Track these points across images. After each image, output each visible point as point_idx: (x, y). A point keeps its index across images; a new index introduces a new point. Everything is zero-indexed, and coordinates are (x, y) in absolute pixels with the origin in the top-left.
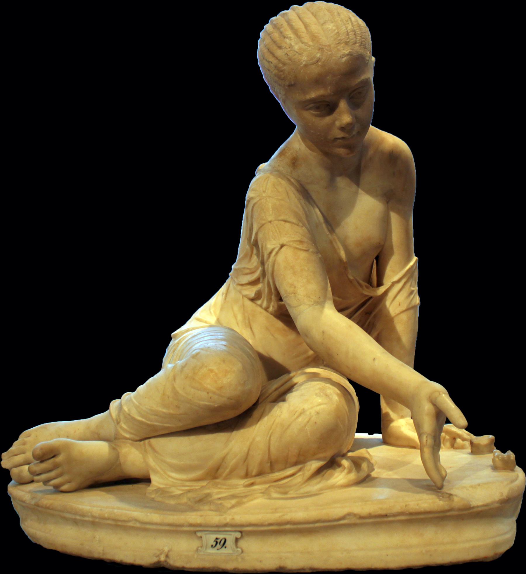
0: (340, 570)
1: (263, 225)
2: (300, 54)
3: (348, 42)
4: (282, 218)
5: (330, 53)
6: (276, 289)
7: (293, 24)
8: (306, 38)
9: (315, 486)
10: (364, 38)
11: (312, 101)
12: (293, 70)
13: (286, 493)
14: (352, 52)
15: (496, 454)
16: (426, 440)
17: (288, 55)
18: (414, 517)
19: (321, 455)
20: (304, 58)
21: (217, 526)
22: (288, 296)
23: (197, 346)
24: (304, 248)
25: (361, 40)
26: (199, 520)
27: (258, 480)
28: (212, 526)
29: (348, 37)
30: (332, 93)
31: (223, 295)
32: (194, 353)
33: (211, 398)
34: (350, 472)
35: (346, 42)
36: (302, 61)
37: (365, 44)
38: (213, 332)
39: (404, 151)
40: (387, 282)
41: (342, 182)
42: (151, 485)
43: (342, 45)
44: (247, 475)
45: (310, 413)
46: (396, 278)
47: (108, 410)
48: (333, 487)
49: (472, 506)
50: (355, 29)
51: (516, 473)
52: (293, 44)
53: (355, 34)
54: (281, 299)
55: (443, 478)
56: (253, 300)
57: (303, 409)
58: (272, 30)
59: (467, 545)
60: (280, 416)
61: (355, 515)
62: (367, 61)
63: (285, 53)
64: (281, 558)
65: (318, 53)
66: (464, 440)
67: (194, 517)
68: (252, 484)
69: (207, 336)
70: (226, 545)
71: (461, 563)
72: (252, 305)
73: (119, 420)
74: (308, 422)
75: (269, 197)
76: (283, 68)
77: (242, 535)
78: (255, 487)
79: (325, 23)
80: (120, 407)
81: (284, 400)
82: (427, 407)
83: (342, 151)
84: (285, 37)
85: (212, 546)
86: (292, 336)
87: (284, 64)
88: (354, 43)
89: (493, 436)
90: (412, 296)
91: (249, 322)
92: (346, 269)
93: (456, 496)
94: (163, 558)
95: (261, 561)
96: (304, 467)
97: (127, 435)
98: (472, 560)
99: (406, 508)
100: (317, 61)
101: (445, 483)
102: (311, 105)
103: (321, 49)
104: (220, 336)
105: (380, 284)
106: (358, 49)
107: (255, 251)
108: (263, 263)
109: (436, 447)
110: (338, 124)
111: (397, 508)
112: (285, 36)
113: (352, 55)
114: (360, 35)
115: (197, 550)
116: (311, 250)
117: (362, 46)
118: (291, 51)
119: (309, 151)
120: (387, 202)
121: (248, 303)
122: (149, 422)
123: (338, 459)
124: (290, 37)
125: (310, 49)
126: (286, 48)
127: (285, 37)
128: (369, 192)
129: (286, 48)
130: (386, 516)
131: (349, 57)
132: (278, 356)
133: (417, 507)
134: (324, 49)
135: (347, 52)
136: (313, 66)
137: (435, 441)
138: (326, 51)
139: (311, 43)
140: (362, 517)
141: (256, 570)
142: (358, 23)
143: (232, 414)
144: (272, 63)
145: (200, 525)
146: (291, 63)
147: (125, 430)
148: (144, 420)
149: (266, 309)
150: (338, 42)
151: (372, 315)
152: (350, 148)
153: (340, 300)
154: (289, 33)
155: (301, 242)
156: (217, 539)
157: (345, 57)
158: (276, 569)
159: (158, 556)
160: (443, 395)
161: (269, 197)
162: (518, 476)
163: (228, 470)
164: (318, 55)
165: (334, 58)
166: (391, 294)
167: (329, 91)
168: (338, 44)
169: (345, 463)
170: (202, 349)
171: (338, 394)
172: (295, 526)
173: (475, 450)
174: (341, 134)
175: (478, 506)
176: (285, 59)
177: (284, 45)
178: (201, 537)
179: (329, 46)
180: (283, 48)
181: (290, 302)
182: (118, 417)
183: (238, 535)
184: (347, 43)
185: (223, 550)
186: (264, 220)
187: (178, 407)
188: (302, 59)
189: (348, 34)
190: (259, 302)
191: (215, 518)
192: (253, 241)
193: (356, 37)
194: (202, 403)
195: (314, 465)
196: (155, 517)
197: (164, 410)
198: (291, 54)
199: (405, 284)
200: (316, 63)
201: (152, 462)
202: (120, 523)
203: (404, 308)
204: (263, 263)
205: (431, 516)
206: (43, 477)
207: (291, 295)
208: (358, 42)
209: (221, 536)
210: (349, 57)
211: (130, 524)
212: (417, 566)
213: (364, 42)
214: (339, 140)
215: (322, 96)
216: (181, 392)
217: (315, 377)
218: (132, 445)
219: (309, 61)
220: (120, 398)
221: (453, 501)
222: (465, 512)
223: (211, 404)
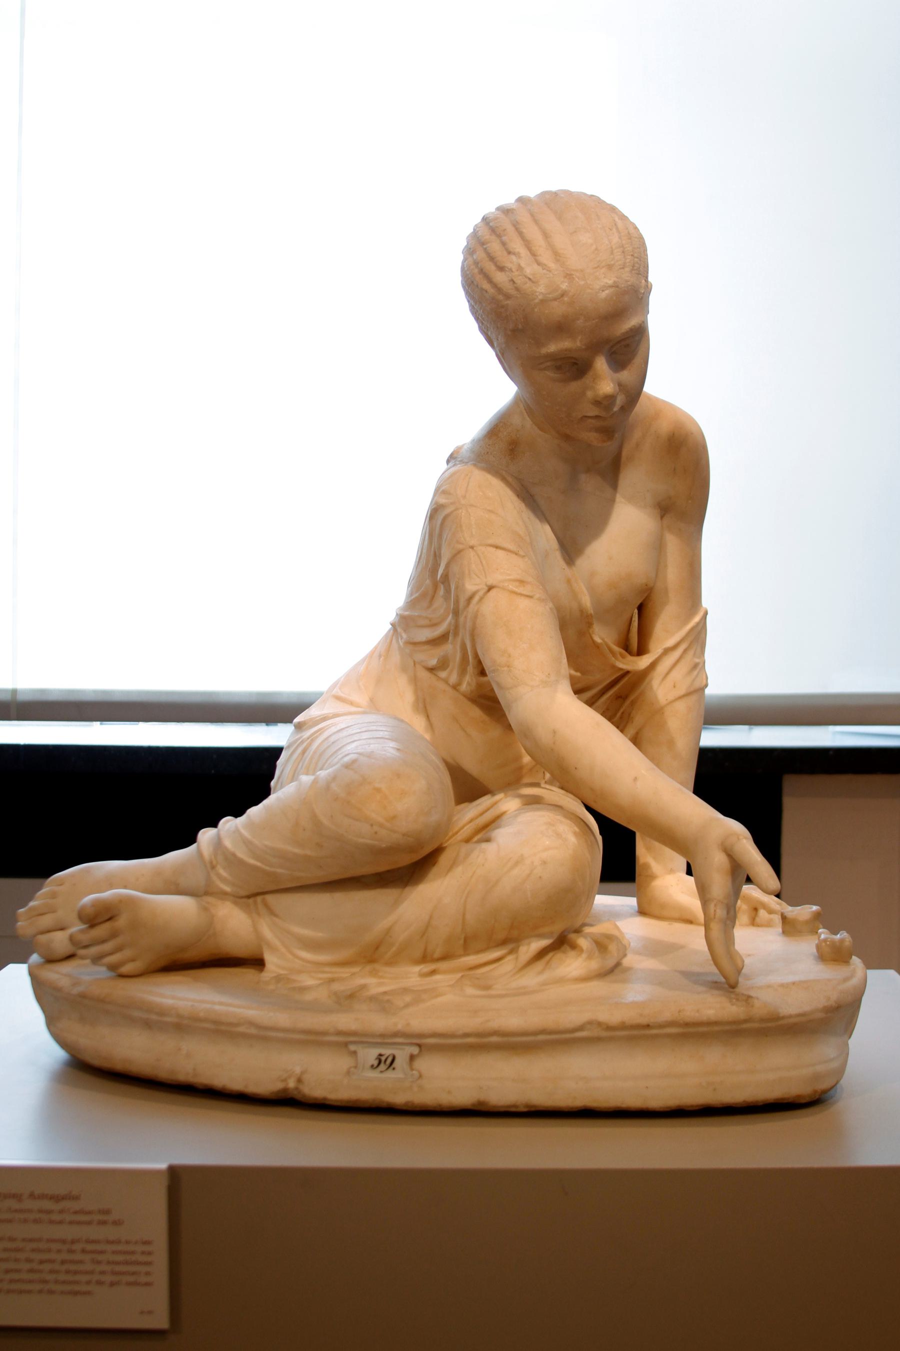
0: (572, 1108)
1: (460, 552)
2: (533, 282)
3: (613, 265)
4: (490, 542)
5: (582, 283)
6: (476, 656)
7: (524, 231)
8: (546, 257)
9: (531, 979)
10: (637, 258)
11: (552, 357)
12: (522, 306)
13: (488, 988)
15: (823, 936)
16: (715, 911)
17: (514, 282)
18: (691, 1030)
19: (546, 930)
20: (541, 290)
21: (382, 1036)
22: (498, 670)
23: (350, 748)
24: (525, 593)
25: (632, 261)
26: (354, 1026)
27: (443, 965)
28: (373, 1035)
29: (612, 256)
30: (584, 347)
31: (380, 659)
32: (346, 759)
33: (376, 833)
34: (590, 957)
35: (609, 265)
36: (537, 294)
37: (639, 268)
38: (373, 724)
39: (692, 434)
40: (656, 649)
41: (589, 483)
42: (266, 969)
43: (603, 270)
44: (424, 958)
45: (532, 863)
46: (670, 642)
47: (194, 846)
48: (561, 981)
49: (781, 1015)
50: (624, 242)
51: (853, 967)
52: (523, 264)
53: (623, 252)
54: (483, 673)
55: (739, 971)
56: (431, 670)
57: (522, 855)
58: (487, 237)
60: (483, 865)
61: (599, 1024)
62: (642, 295)
63: (510, 279)
64: (481, 1088)
65: (563, 282)
66: (771, 912)
67: (345, 1021)
68: (433, 972)
69: (366, 731)
70: (395, 1065)
71: (761, 1104)
72: (430, 678)
73: (214, 862)
74: (529, 875)
75: (472, 505)
76: (506, 303)
77: (420, 1051)
78: (437, 977)
79: (575, 232)
80: (218, 843)
81: (488, 840)
82: (719, 859)
83: (592, 437)
84: (509, 253)
85: (372, 1066)
86: (496, 732)
87: (508, 297)
88: (621, 267)
89: (818, 907)
90: (695, 673)
91: (425, 707)
92: (590, 625)
93: (758, 999)
94: (291, 1084)
95: (449, 1092)
96: (518, 947)
97: (227, 889)
98: (777, 1099)
99: (679, 1014)
100: (562, 295)
101: (740, 979)
102: (548, 364)
103: (569, 276)
104: (381, 733)
105: (641, 650)
106: (628, 277)
107: (441, 591)
108: (456, 613)
109: (728, 922)
110: (590, 394)
111: (666, 1016)
112: (512, 250)
113: (617, 287)
114: (632, 253)
115: (348, 1073)
116: (537, 596)
117: (633, 272)
118: (519, 275)
119: (540, 432)
120: (662, 517)
121: (424, 674)
122: (267, 868)
123: (572, 936)
124: (519, 253)
125: (551, 275)
126: (512, 271)
127: (509, 253)
129: (511, 270)
130: (648, 1026)
131: (612, 290)
132: (471, 764)
133: (697, 1014)
134: (574, 276)
135: (610, 282)
136: (556, 303)
137: (728, 913)
138: (577, 279)
139: (552, 265)
140: (609, 1028)
141: (440, 1105)
142: (629, 233)
143: (406, 860)
144: (486, 291)
145: (354, 1033)
146: (518, 296)
147: (224, 880)
148: (259, 864)
149: (455, 687)
150: (596, 266)
151: (628, 702)
152: (608, 432)
153: (578, 674)
154: (517, 246)
155: (522, 582)
156: (381, 1055)
158: (473, 1105)
159: (285, 1080)
160: (745, 841)
161: (472, 505)
162: (854, 971)
163: (394, 949)
164: (564, 286)
165: (590, 291)
166: (662, 668)
167: (578, 344)
168: (596, 268)
169: (583, 942)
170: (360, 754)
171: (575, 833)
172: (505, 1039)
173: (789, 927)
174: (594, 411)
175: (790, 1016)
176: (508, 287)
177: (509, 265)
178: (355, 1053)
179: (582, 271)
180: (507, 269)
181: (500, 679)
182: (213, 857)
183: (415, 1050)
184: (610, 267)
185: (390, 1074)
186: (462, 544)
187: (319, 845)
188: (538, 290)
189: (612, 253)
190: (443, 674)
191: (379, 1023)
192: (441, 576)
193: (624, 256)
194: (361, 840)
195: (537, 945)
196: (282, 1019)
197: (297, 850)
198: (519, 281)
199: (685, 651)
200: (559, 299)
201: (267, 932)
202: (223, 1028)
203: (682, 691)
204: (456, 613)
205: (716, 1028)
206: (94, 950)
207: (503, 669)
208: (628, 264)
209: (387, 1052)
210: (612, 290)
211: (241, 1029)
212: (692, 1106)
213: (638, 263)
214: (590, 420)
215: (566, 350)
216: (325, 821)
217: (534, 802)
218: (235, 903)
219: (549, 294)
220: (215, 825)
221: (752, 1006)
222: (769, 1025)
223: (375, 843)
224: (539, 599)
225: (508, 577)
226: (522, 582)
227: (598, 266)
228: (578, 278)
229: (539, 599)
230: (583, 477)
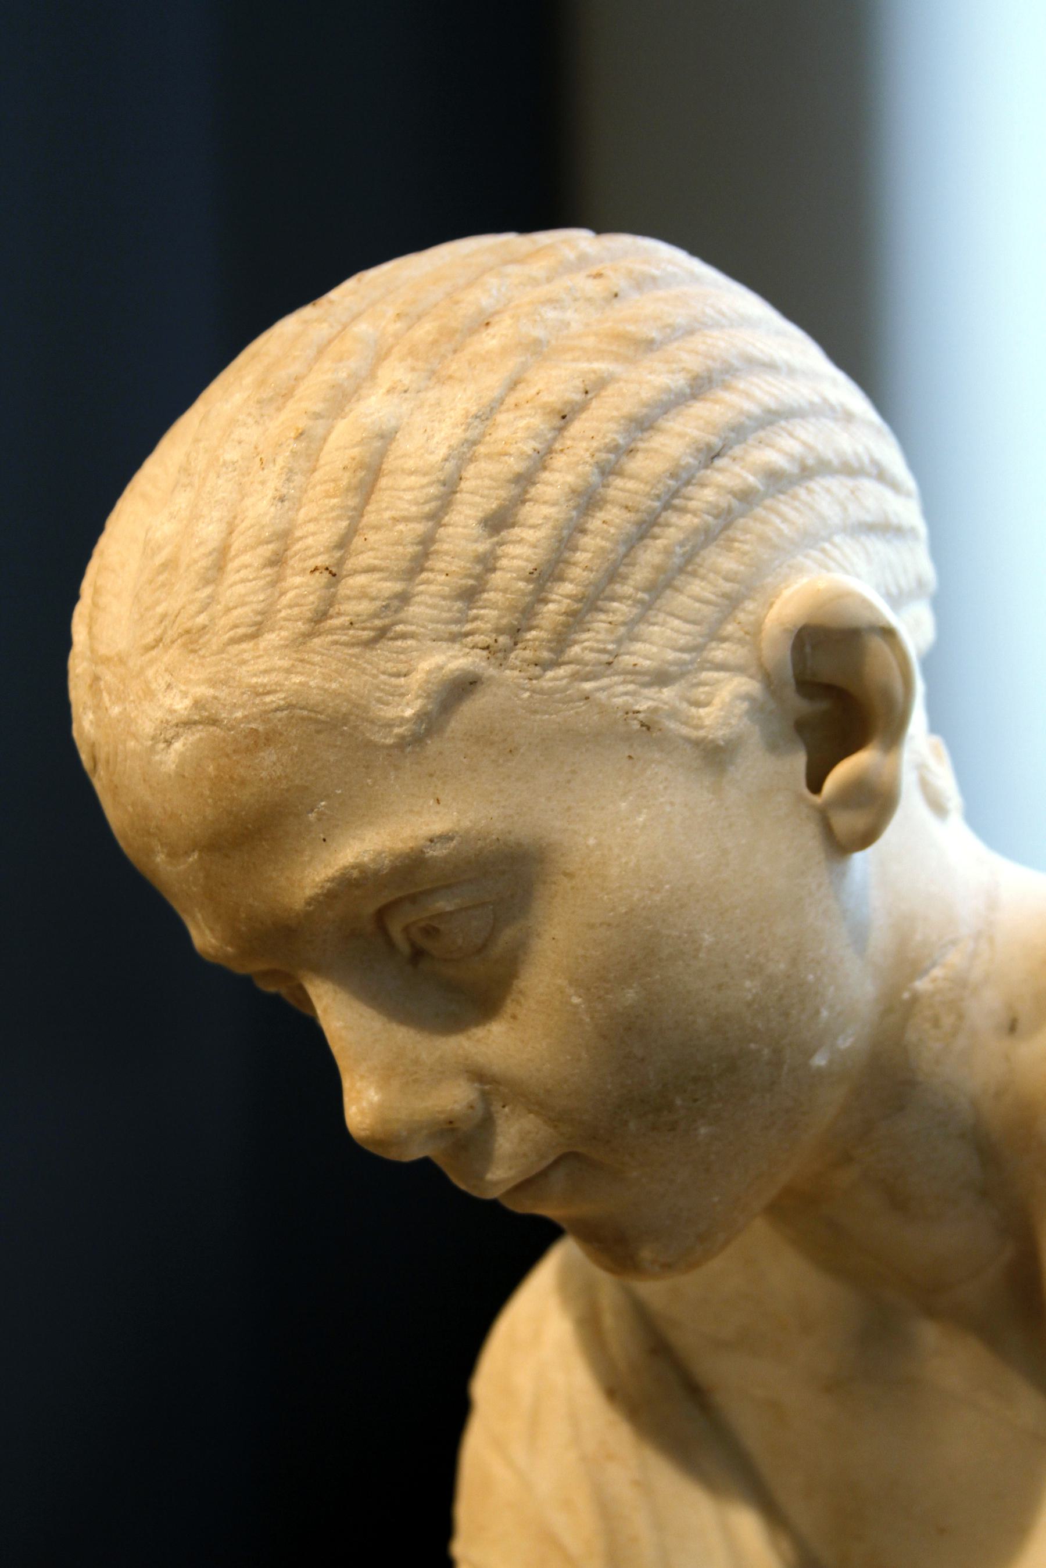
14: (215, 698)
43: (174, 652)
106: (266, 672)
113: (214, 722)
135: (181, 706)
150: (150, 638)
157: (177, 736)
179: (122, 661)
208: (283, 614)
227: (159, 641)
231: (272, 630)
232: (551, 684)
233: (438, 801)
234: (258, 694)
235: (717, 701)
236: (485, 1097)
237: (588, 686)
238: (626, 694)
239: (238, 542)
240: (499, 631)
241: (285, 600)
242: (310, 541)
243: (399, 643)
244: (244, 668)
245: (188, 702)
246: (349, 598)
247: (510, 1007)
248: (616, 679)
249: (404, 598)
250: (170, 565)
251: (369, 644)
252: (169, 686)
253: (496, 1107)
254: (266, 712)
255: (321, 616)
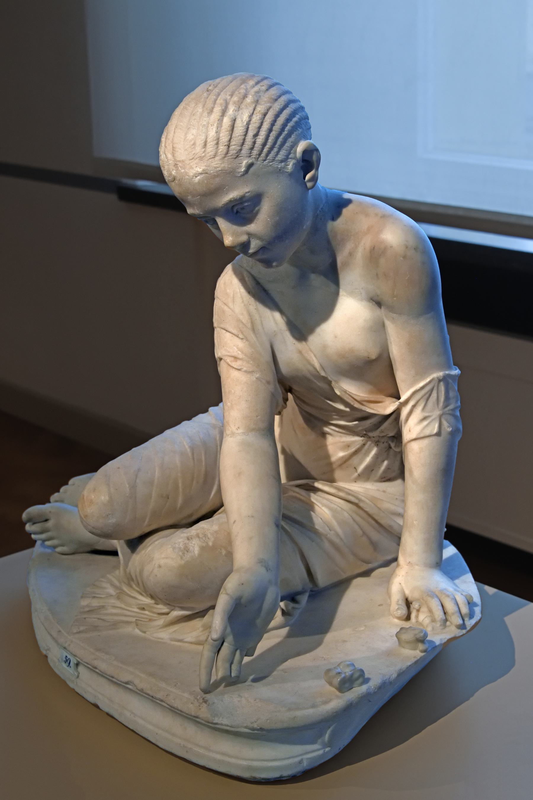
5: (183, 171)
24: (235, 366)
29: (203, 150)
41: (316, 280)
43: (197, 161)
59: (218, 757)
90: (425, 423)
106: (217, 164)
113: (207, 173)
116: (245, 369)
128: (351, 294)
134: (178, 166)
135: (200, 170)
150: (191, 158)
153: (348, 409)
157: (199, 176)
165: (187, 177)
179: (183, 161)
184: (201, 158)
195: (177, 613)
208: (219, 153)
224: (246, 371)
225: (228, 354)
226: (236, 358)
227: (193, 158)
228: (181, 167)
229: (246, 371)
230: (313, 276)
231: (217, 157)
232: (265, 164)
233: (247, 186)
234: (215, 168)
235: (290, 165)
236: (249, 237)
237: (271, 163)
238: (276, 165)
239: (209, 140)
240: (256, 155)
241: (220, 150)
242: (223, 140)
243: (240, 158)
244: (213, 163)
245: (201, 170)
246: (231, 150)
247: (255, 221)
248: (275, 162)
249: (241, 150)
250: (194, 144)
251: (236, 158)
252: (196, 167)
253: (251, 239)
254: (217, 171)
255: (227, 153)
